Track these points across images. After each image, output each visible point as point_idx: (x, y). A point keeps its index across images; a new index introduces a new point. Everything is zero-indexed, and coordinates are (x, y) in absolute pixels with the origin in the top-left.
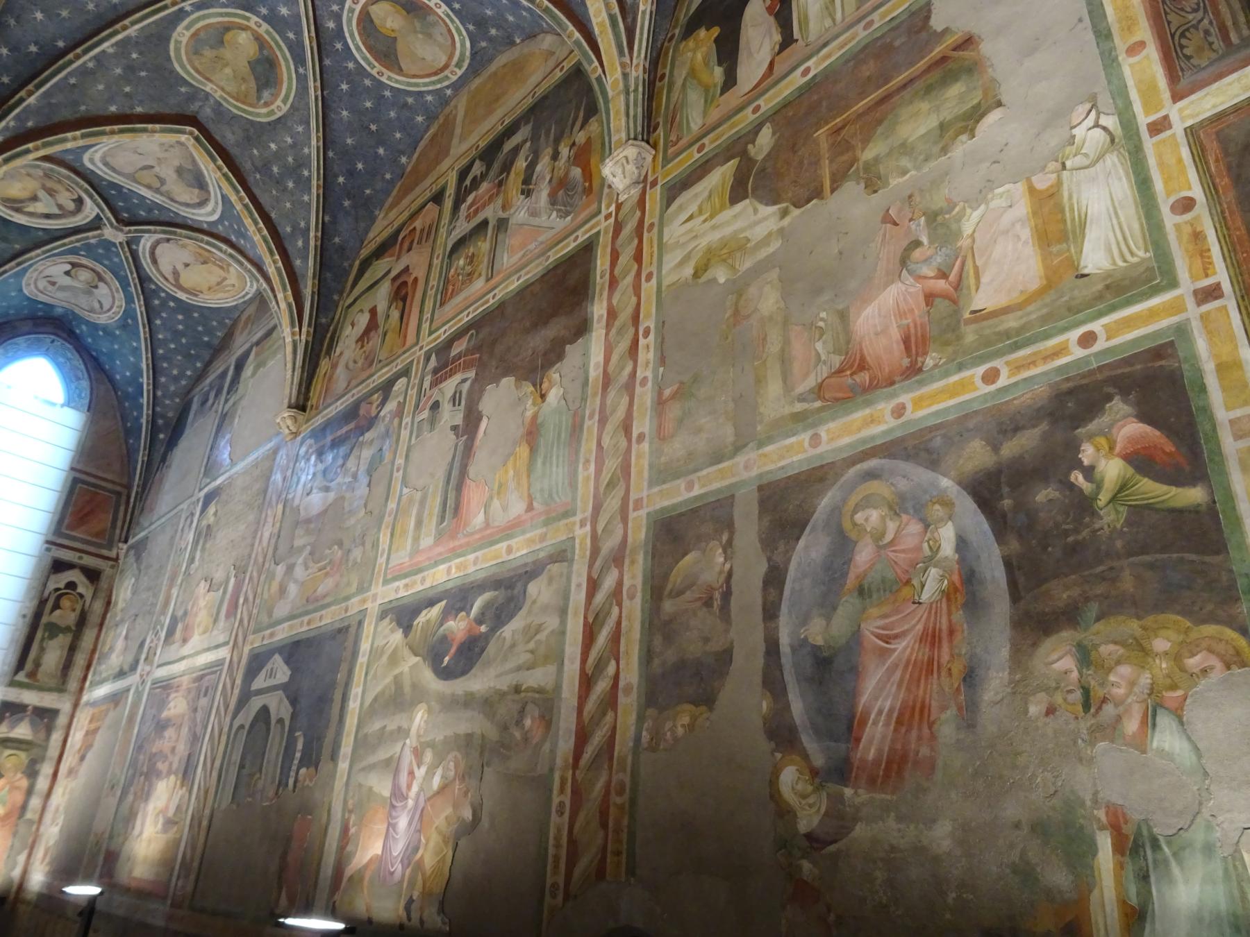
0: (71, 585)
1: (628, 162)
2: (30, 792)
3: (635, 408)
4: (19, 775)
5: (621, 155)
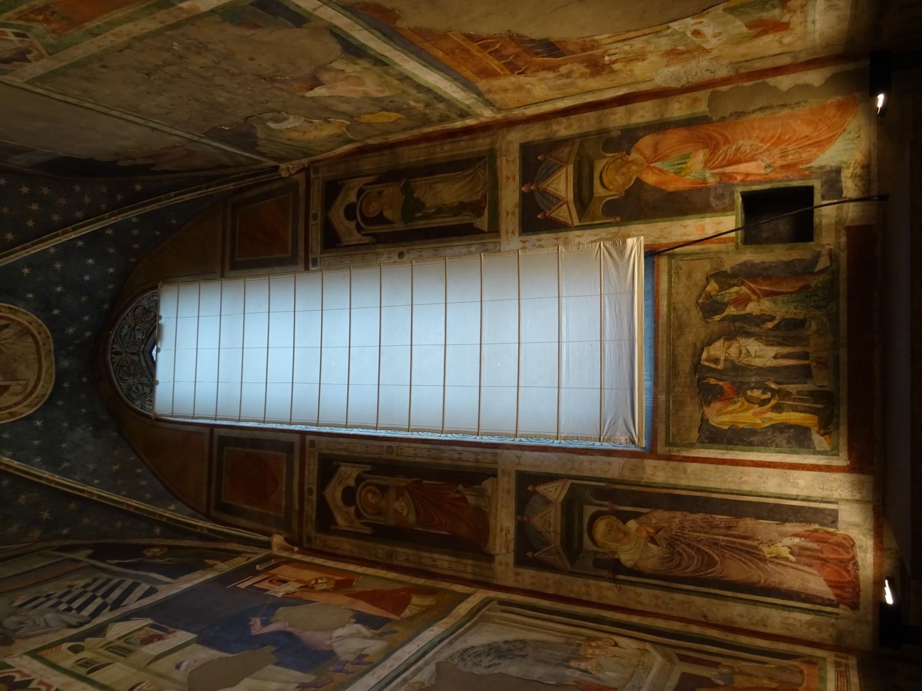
0: (350, 212)
2: (660, 127)
4: (634, 156)
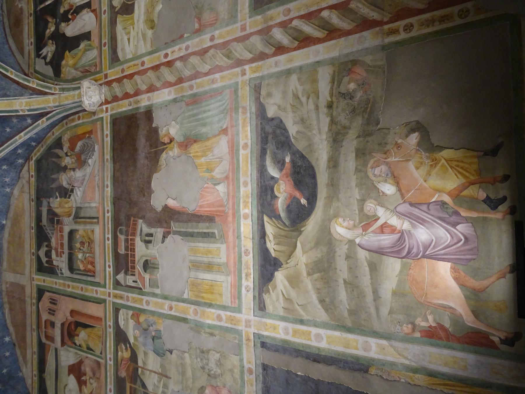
1: (90, 88)
3: (197, 49)
5: (84, 90)
